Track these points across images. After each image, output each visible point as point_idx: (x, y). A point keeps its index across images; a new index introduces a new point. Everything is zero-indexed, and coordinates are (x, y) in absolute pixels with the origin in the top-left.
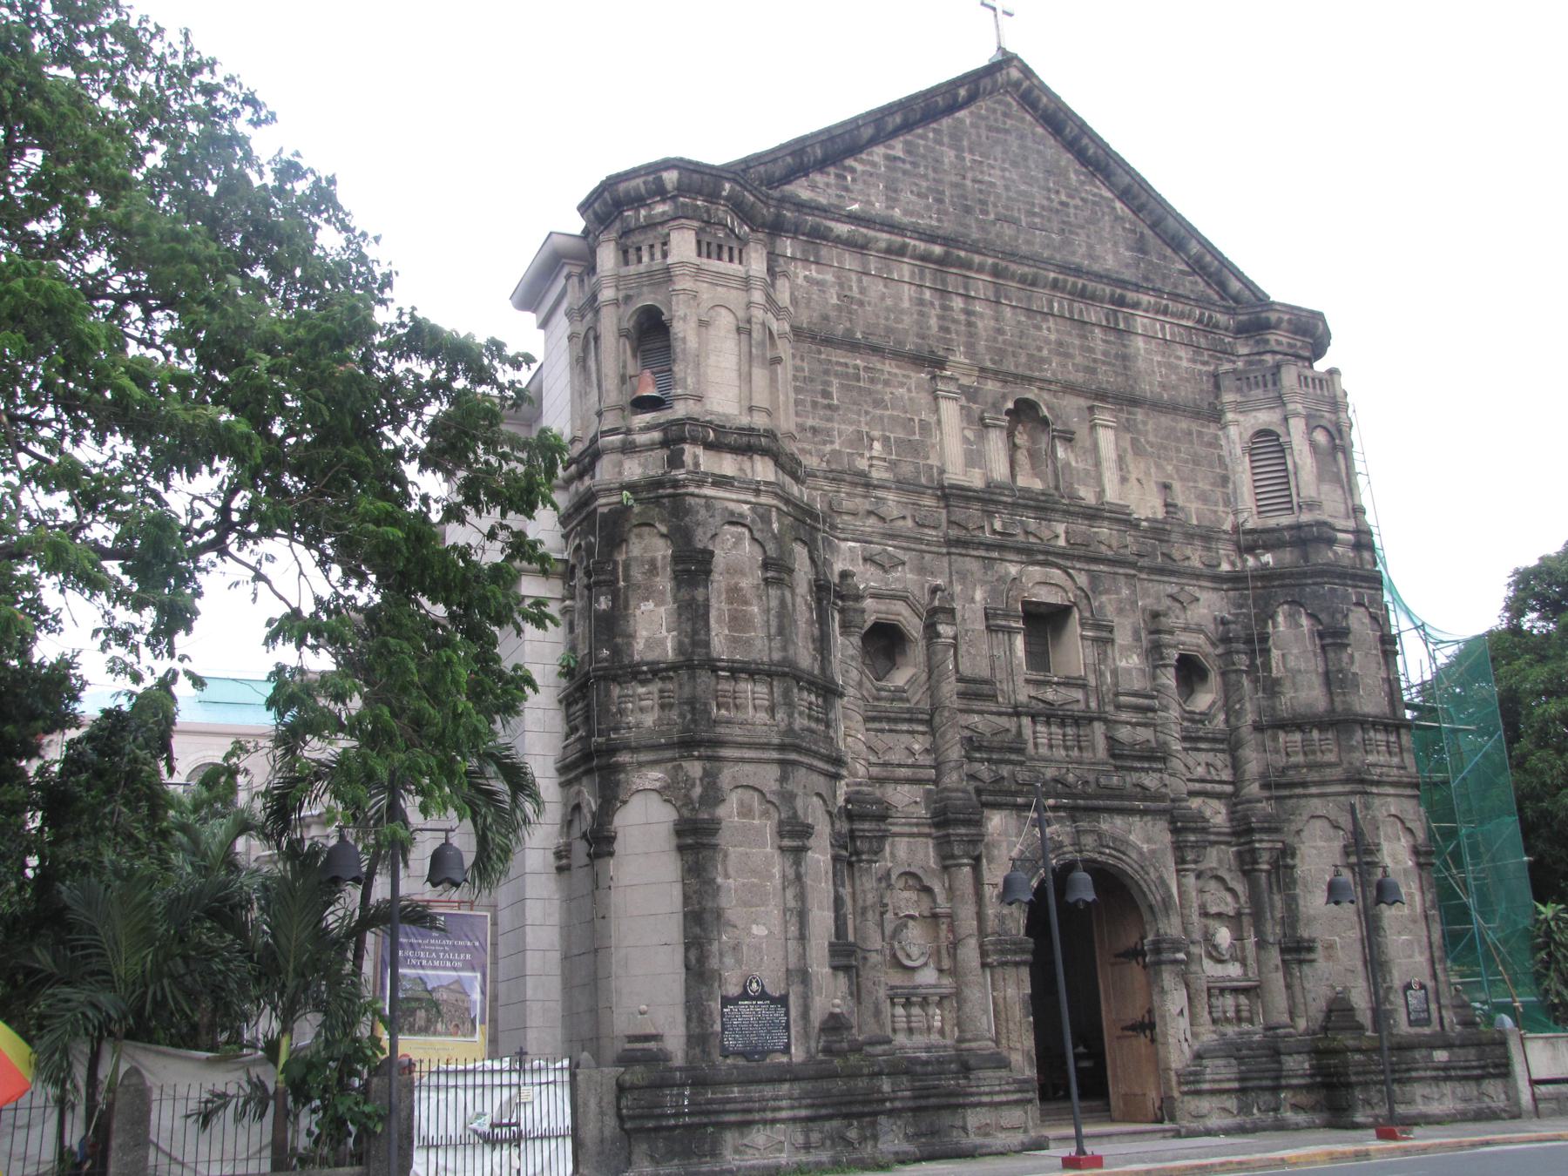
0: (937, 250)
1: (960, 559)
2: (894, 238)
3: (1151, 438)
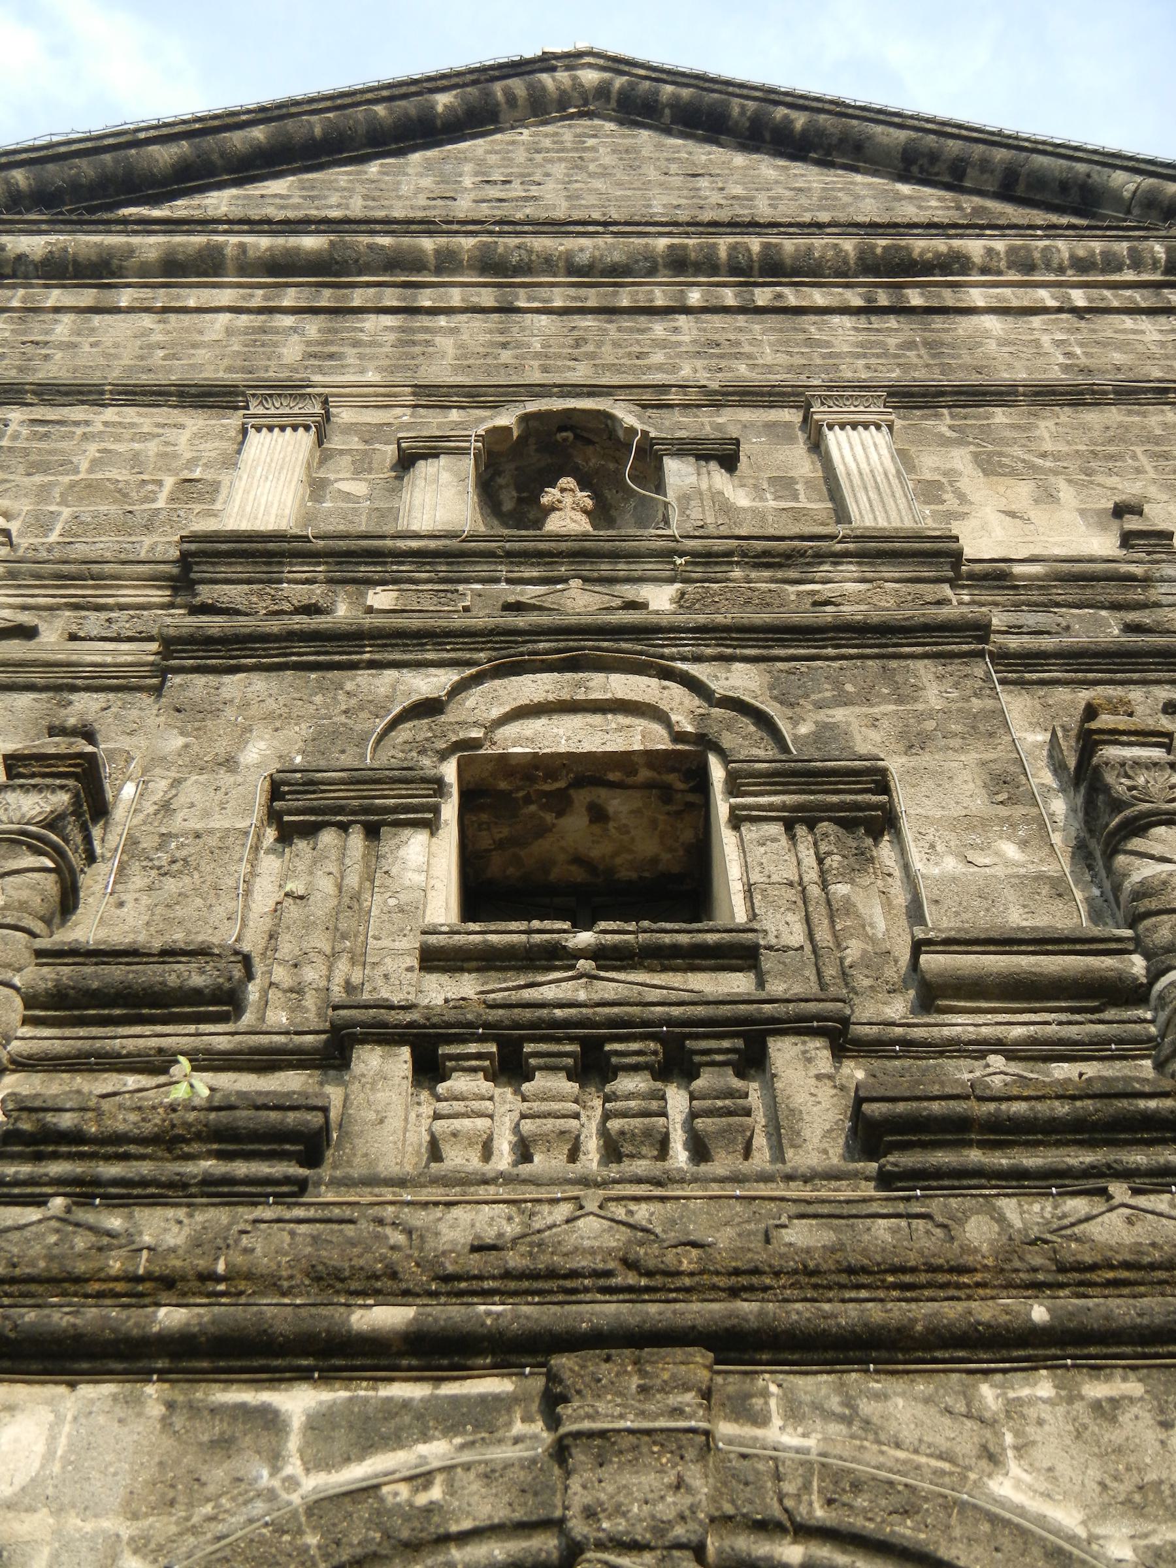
0: (311, 242)
1: (200, 680)
2: (178, 239)
3: (1048, 446)
